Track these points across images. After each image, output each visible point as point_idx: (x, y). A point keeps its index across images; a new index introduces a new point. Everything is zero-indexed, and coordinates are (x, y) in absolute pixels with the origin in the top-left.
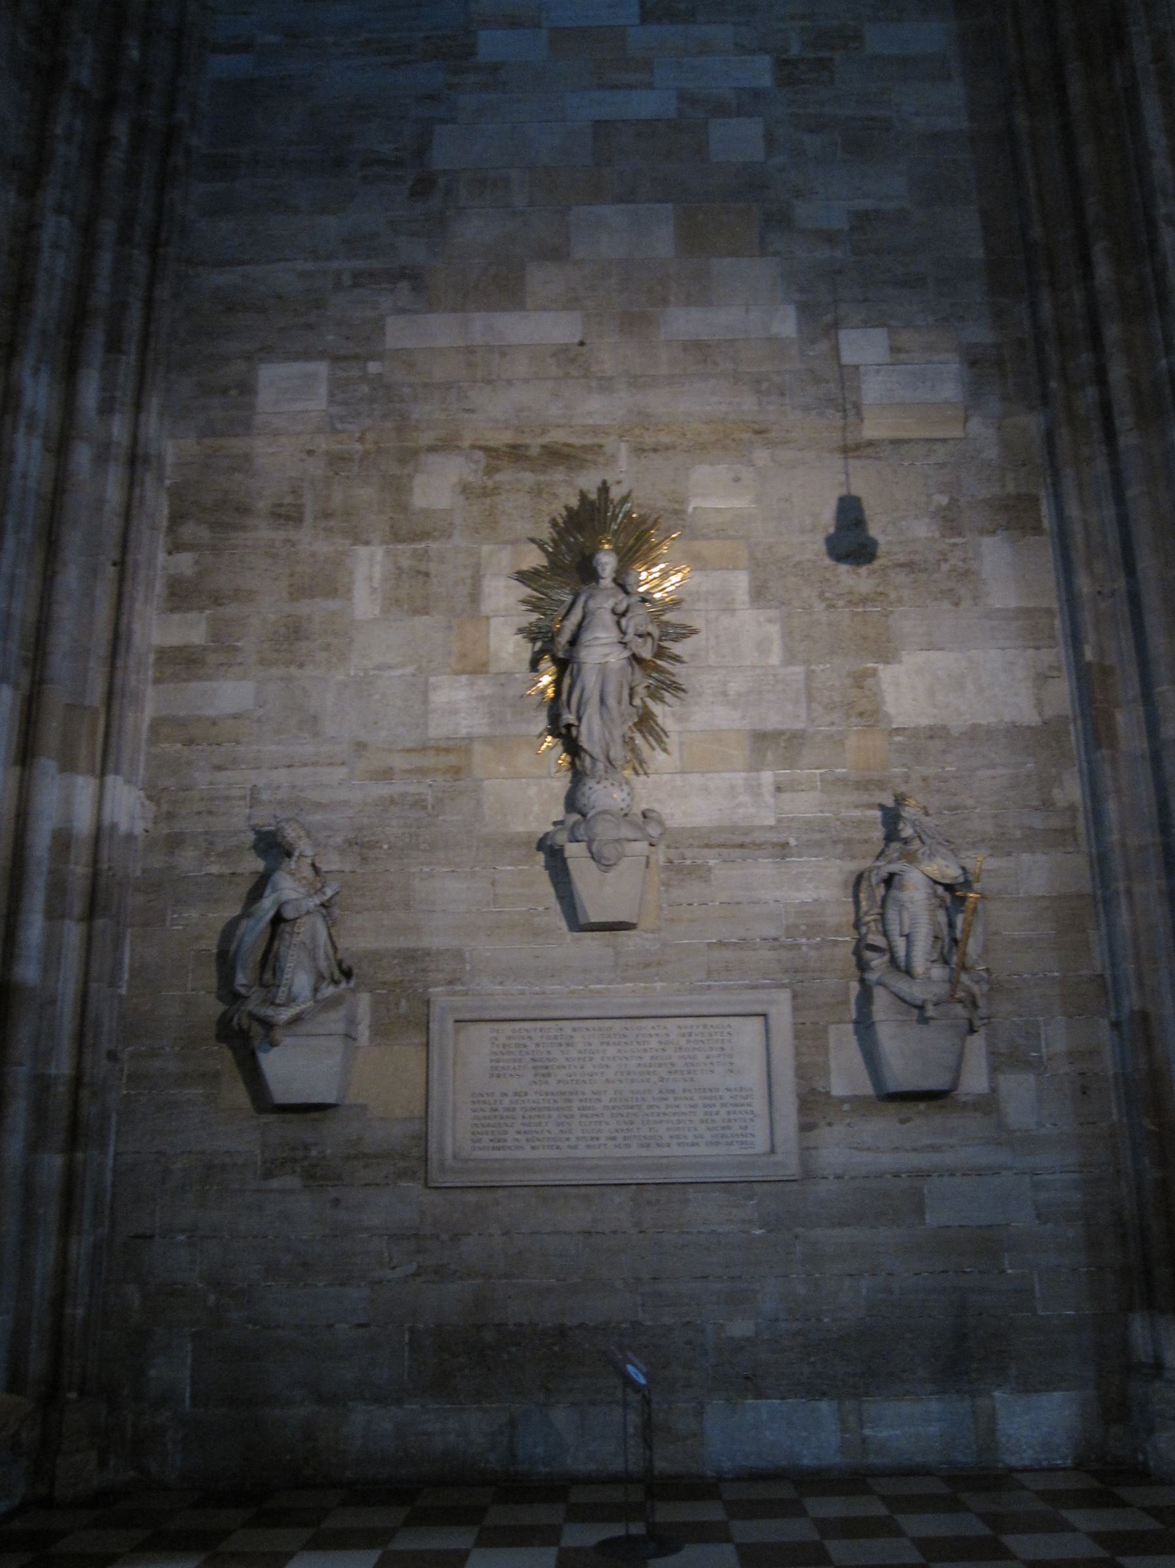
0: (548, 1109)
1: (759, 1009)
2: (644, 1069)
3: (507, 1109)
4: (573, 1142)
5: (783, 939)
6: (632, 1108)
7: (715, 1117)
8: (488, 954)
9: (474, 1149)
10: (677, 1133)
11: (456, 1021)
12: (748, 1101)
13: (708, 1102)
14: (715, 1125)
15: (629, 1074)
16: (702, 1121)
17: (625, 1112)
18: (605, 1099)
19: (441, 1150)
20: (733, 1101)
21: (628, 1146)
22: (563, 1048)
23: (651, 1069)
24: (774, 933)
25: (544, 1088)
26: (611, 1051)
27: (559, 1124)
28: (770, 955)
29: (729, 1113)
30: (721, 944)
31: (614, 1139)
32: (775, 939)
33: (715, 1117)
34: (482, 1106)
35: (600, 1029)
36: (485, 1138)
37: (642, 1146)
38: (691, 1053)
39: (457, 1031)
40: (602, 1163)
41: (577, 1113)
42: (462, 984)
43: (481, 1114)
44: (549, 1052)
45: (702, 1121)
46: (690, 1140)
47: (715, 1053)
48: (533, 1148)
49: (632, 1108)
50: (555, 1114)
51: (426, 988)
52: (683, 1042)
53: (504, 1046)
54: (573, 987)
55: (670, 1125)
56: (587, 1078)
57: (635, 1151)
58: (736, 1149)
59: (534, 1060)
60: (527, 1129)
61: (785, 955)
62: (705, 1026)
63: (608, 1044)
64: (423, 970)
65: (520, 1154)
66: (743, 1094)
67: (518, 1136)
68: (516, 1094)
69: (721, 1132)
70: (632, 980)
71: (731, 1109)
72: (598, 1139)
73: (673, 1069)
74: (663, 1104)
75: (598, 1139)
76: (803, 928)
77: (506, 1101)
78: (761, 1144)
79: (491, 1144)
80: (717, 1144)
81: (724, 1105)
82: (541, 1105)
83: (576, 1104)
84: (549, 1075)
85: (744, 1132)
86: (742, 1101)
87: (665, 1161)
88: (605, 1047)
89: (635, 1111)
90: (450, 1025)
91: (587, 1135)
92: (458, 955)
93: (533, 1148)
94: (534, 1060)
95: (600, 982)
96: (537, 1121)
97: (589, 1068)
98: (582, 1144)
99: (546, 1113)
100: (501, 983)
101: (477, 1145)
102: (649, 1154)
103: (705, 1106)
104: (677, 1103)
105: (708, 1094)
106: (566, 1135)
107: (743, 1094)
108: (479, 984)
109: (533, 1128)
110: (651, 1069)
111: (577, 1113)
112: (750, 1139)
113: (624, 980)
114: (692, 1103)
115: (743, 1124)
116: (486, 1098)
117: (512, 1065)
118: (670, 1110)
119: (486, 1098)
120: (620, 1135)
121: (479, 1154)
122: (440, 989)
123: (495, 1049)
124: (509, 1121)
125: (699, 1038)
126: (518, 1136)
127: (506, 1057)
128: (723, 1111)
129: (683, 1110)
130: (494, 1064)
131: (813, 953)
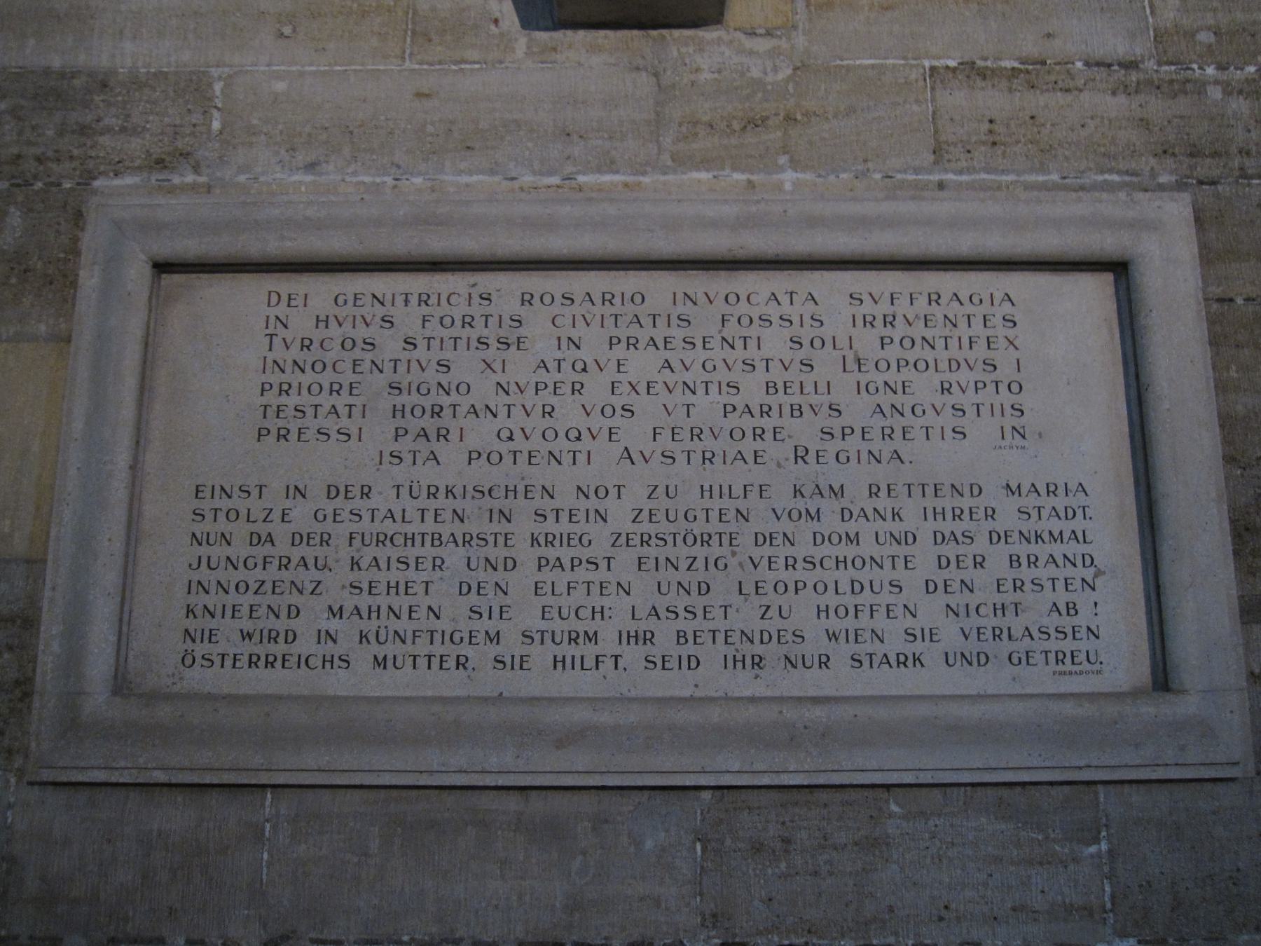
0: (437, 539)
1: (1106, 243)
2: (748, 423)
3: (298, 538)
4: (512, 645)
5: (1151, 65)
6: (706, 540)
7: (970, 574)
8: (280, 86)
9: (188, 660)
10: (850, 623)
11: (162, 267)
12: (1078, 524)
13: (947, 526)
14: (974, 600)
15: (695, 434)
16: (930, 587)
17: (682, 552)
18: (620, 514)
19: (73, 661)
20: (1028, 526)
21: (694, 663)
22: (491, 353)
23: (768, 423)
24: (1116, 45)
25: (426, 474)
26: (642, 364)
27: (464, 589)
28: (1115, 105)
29: (1014, 561)
30: (972, 71)
31: (647, 638)
32: (1130, 65)
33: (970, 574)
34: (222, 525)
35: (608, 299)
36: (228, 628)
37: (738, 662)
38: (892, 376)
39: (157, 302)
40: (604, 718)
41: (527, 555)
42: (196, 169)
43: (218, 552)
44: (444, 366)
45: (930, 587)
46: (895, 645)
47: (964, 376)
48: (380, 662)
49: (706, 540)
50: (455, 557)
51: (90, 176)
52: (867, 341)
53: (306, 345)
54: (528, 179)
55: (830, 599)
56: (562, 445)
57: (715, 678)
58: (1040, 678)
59: (395, 387)
60: (364, 601)
61: (1156, 107)
62: (934, 299)
63: (632, 344)
64: (83, 130)
65: (337, 683)
66: (1060, 502)
67: (334, 625)
68: (332, 491)
69: (990, 622)
70: (705, 163)
71: (1022, 549)
72: (592, 638)
73: (836, 424)
74: (804, 530)
75: (592, 638)
76: (1205, 37)
77: (301, 514)
78: (1122, 657)
79: (247, 648)
80: (983, 659)
81: (996, 537)
82: (414, 528)
83: (523, 527)
84: (442, 435)
85: (1066, 622)
86: (1056, 526)
87: (819, 712)
88: (620, 351)
89: (715, 551)
90: (137, 274)
91: (557, 625)
92: (194, 87)
93: (380, 662)
94: (395, 387)
95: (610, 166)
96: (395, 575)
97: (569, 413)
98: (541, 655)
99: (428, 551)
100: (311, 167)
101: (200, 649)
102: (759, 689)
103: (939, 538)
104: (852, 527)
105: (947, 502)
106: (492, 626)
107: (1060, 502)
108: (242, 169)
109: (383, 601)
110: (768, 423)
111: (527, 555)
112: (1084, 645)
113: (682, 162)
114: (896, 528)
115: (1062, 598)
116: (238, 502)
117: (326, 401)
118: (826, 549)
119: (238, 502)
120: (665, 631)
121: (200, 678)
122: (129, 180)
123: (279, 353)
124: (306, 578)
125: (918, 330)
126: (334, 625)
127: (308, 378)
128: (997, 557)
129: (867, 548)
130: (272, 398)
131: (1240, 105)
